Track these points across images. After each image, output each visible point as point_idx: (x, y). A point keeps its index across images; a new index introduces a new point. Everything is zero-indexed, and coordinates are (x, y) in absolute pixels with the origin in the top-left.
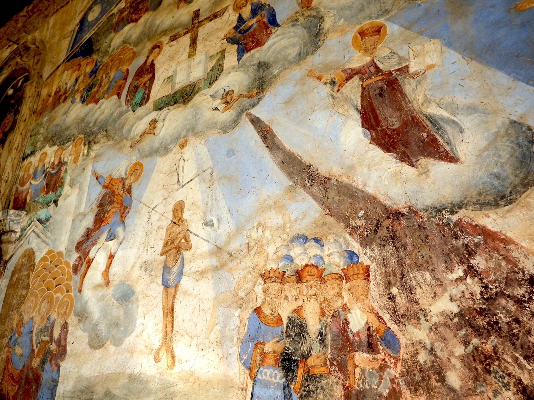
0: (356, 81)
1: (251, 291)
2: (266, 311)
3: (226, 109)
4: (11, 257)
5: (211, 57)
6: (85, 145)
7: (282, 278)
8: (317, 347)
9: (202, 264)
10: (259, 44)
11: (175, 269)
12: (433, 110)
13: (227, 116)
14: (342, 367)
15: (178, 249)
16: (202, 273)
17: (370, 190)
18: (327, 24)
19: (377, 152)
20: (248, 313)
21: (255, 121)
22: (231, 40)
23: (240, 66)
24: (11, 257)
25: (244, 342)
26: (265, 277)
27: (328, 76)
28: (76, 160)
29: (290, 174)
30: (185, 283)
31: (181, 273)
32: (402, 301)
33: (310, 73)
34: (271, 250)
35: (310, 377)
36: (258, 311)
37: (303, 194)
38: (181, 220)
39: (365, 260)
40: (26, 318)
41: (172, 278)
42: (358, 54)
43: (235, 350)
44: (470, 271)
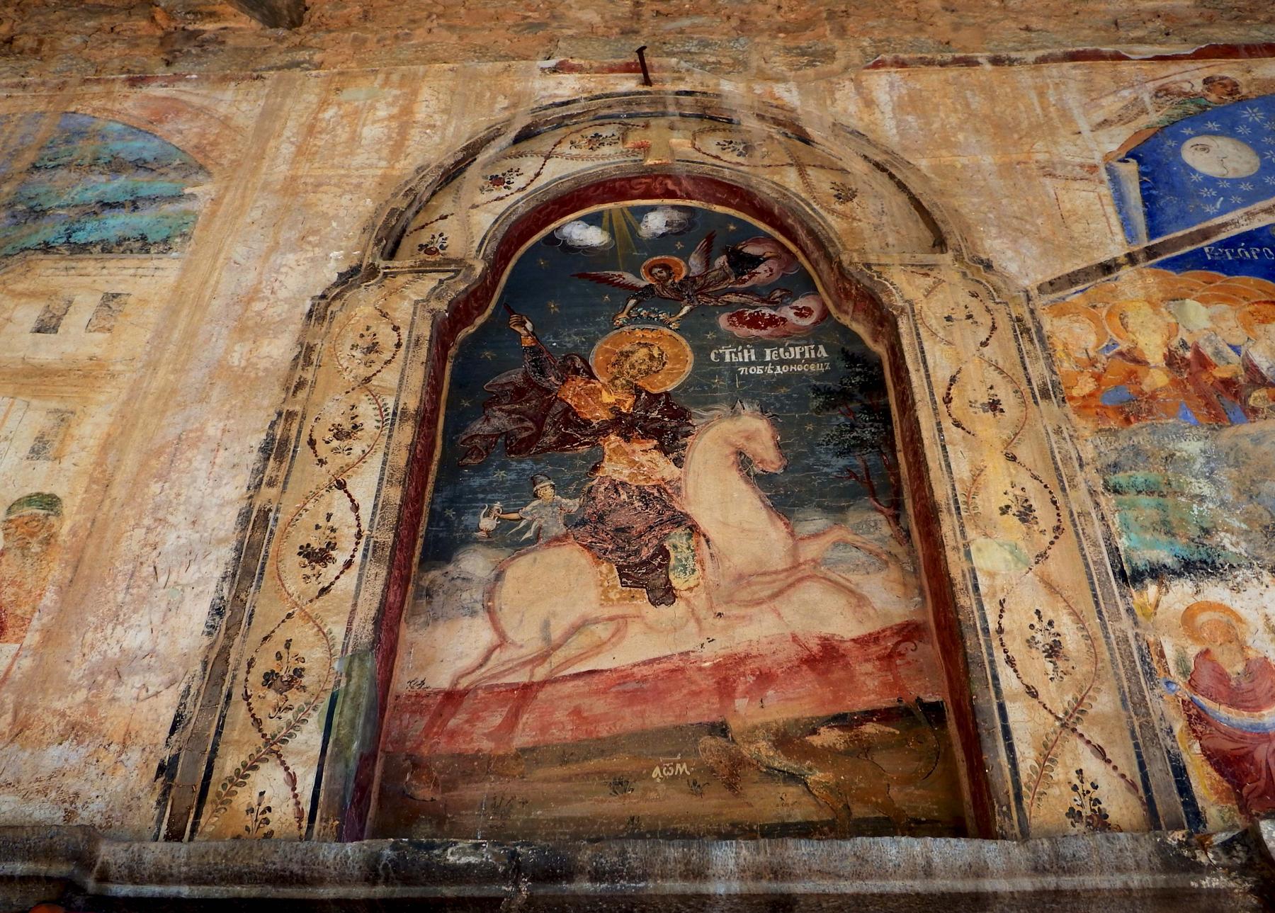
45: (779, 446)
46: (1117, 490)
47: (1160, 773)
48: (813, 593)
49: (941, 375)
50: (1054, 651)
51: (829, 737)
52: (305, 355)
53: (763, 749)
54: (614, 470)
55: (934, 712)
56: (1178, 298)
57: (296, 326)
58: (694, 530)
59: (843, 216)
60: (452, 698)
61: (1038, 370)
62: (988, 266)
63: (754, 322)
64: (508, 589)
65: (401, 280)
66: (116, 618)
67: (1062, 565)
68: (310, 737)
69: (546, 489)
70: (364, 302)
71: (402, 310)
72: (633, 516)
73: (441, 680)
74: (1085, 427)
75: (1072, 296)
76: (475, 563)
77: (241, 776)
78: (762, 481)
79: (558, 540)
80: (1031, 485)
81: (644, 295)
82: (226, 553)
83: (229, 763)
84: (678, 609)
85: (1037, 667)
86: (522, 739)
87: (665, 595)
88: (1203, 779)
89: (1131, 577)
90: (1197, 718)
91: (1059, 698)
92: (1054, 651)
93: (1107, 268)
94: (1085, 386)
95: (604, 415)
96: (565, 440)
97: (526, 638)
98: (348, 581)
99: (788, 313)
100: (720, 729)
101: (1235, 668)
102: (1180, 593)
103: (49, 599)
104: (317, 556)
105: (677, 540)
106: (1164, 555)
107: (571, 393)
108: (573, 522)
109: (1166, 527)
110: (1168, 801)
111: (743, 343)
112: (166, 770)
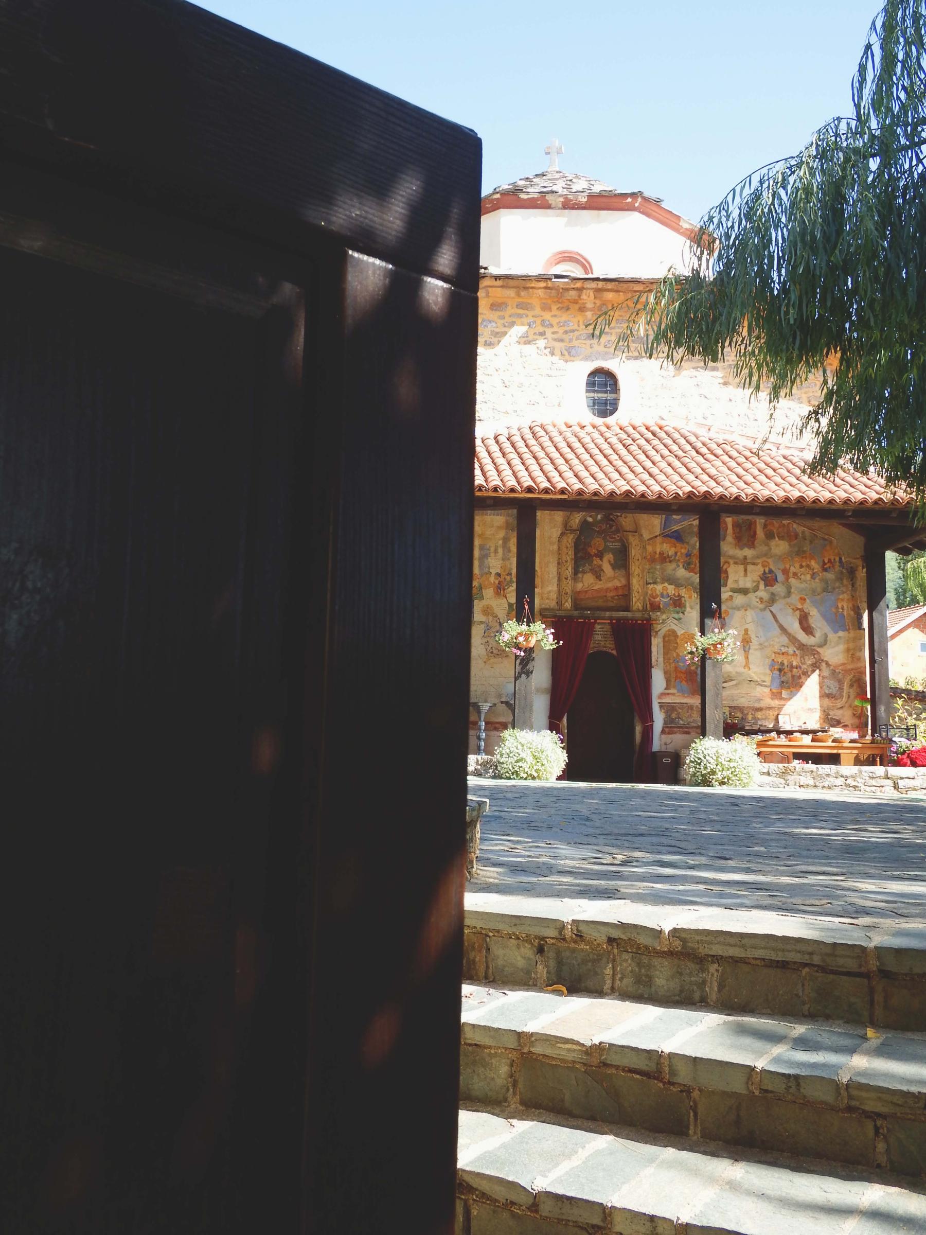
0: (798, 612)
1: (771, 655)
2: (775, 660)
3: (761, 604)
4: (660, 630)
5: (754, 581)
6: (694, 592)
7: (779, 654)
8: (786, 668)
9: (757, 647)
10: (772, 586)
11: (747, 647)
12: (813, 625)
13: (762, 606)
14: (791, 671)
15: (748, 642)
16: (757, 649)
17: (799, 639)
18: (792, 590)
19: (801, 631)
20: (770, 660)
21: (771, 612)
22: (762, 579)
23: (765, 591)
24: (660, 630)
25: (770, 666)
26: (775, 653)
27: (791, 607)
28: (690, 597)
29: (781, 630)
30: (751, 651)
31: (749, 649)
32: (803, 661)
33: (787, 604)
34: (776, 647)
35: (785, 673)
36: (773, 660)
37: (784, 636)
38: (747, 634)
39: (797, 653)
40: (681, 654)
41: (747, 649)
42: (800, 604)
43: (768, 667)
44: (814, 657)
45: (614, 559)
46: (649, 573)
47: (645, 606)
48: (616, 580)
49: (633, 555)
50: (638, 592)
51: (616, 597)
52: (559, 549)
53: (609, 598)
54: (595, 562)
55: (627, 595)
56: (663, 543)
57: (557, 543)
58: (604, 571)
59: (625, 522)
60: (579, 592)
61: (644, 554)
62: (642, 535)
63: (612, 538)
64: (584, 579)
65: (569, 535)
66: (547, 586)
67: (641, 583)
68: (570, 600)
69: (587, 565)
70: (565, 540)
71: (570, 541)
72: (597, 569)
73: (578, 590)
74: (647, 563)
75: (651, 542)
76: (580, 575)
77: (564, 604)
78: (611, 565)
79: (589, 572)
80: (640, 572)
81: (598, 532)
82: (557, 578)
83: (563, 602)
84: (602, 582)
85: (636, 594)
86: (587, 597)
87: (600, 580)
88: (648, 606)
89: (648, 584)
90: (649, 600)
91: (638, 598)
92: (638, 592)
93: (656, 537)
94: (649, 557)
95: (593, 554)
96: (589, 558)
97: (586, 585)
98: (570, 582)
99: (616, 536)
100: (606, 596)
101: (654, 595)
102: (651, 586)
103: (540, 583)
104: (566, 579)
105: (602, 573)
106: (651, 581)
107: (589, 549)
108: (591, 570)
109: (653, 578)
110: (645, 608)
111: (610, 542)
112: (557, 603)
